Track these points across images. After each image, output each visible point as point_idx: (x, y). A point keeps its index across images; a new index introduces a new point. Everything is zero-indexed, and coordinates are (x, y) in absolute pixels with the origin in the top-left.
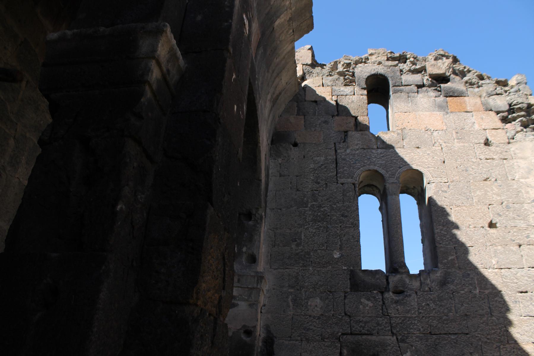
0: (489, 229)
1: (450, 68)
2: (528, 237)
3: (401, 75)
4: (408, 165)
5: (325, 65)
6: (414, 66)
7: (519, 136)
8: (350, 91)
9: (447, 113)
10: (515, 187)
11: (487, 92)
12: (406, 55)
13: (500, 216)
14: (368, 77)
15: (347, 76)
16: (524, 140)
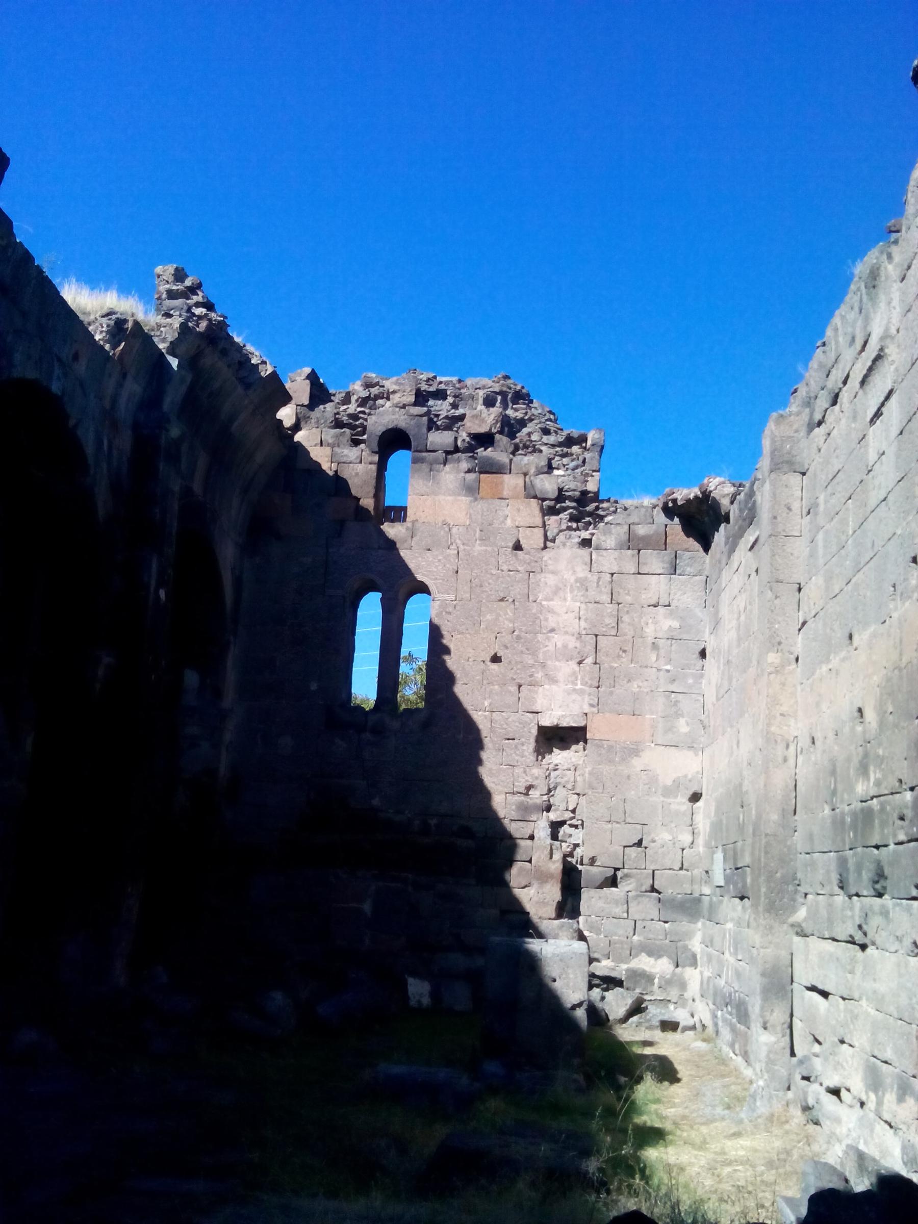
0: (489, 663)
1: (497, 422)
2: (531, 676)
3: (429, 429)
4: (412, 574)
5: (334, 395)
6: (453, 411)
7: (561, 538)
8: (354, 457)
9: (476, 499)
10: (534, 611)
11: (537, 468)
12: (446, 390)
13: (506, 647)
14: (384, 433)
15: (361, 421)
16: (564, 544)
